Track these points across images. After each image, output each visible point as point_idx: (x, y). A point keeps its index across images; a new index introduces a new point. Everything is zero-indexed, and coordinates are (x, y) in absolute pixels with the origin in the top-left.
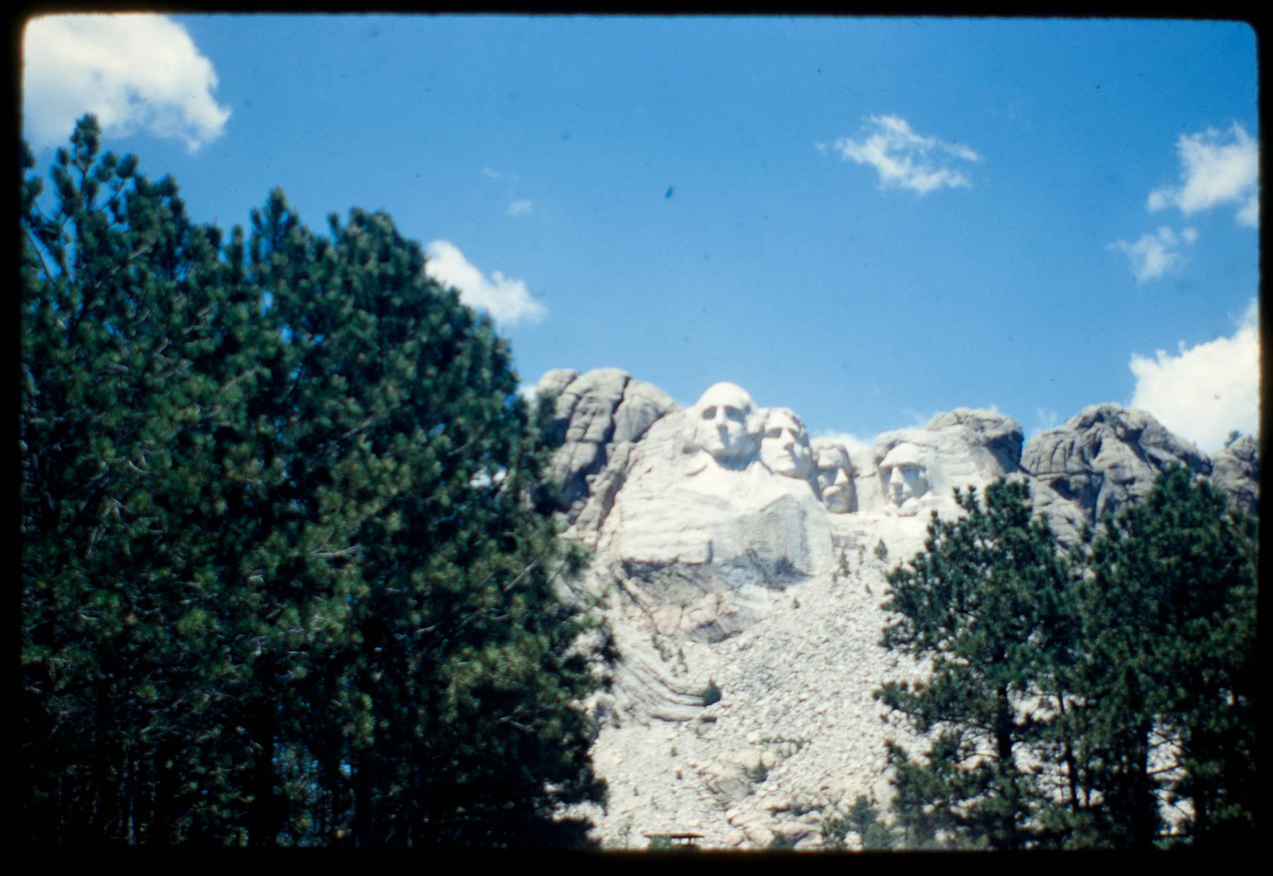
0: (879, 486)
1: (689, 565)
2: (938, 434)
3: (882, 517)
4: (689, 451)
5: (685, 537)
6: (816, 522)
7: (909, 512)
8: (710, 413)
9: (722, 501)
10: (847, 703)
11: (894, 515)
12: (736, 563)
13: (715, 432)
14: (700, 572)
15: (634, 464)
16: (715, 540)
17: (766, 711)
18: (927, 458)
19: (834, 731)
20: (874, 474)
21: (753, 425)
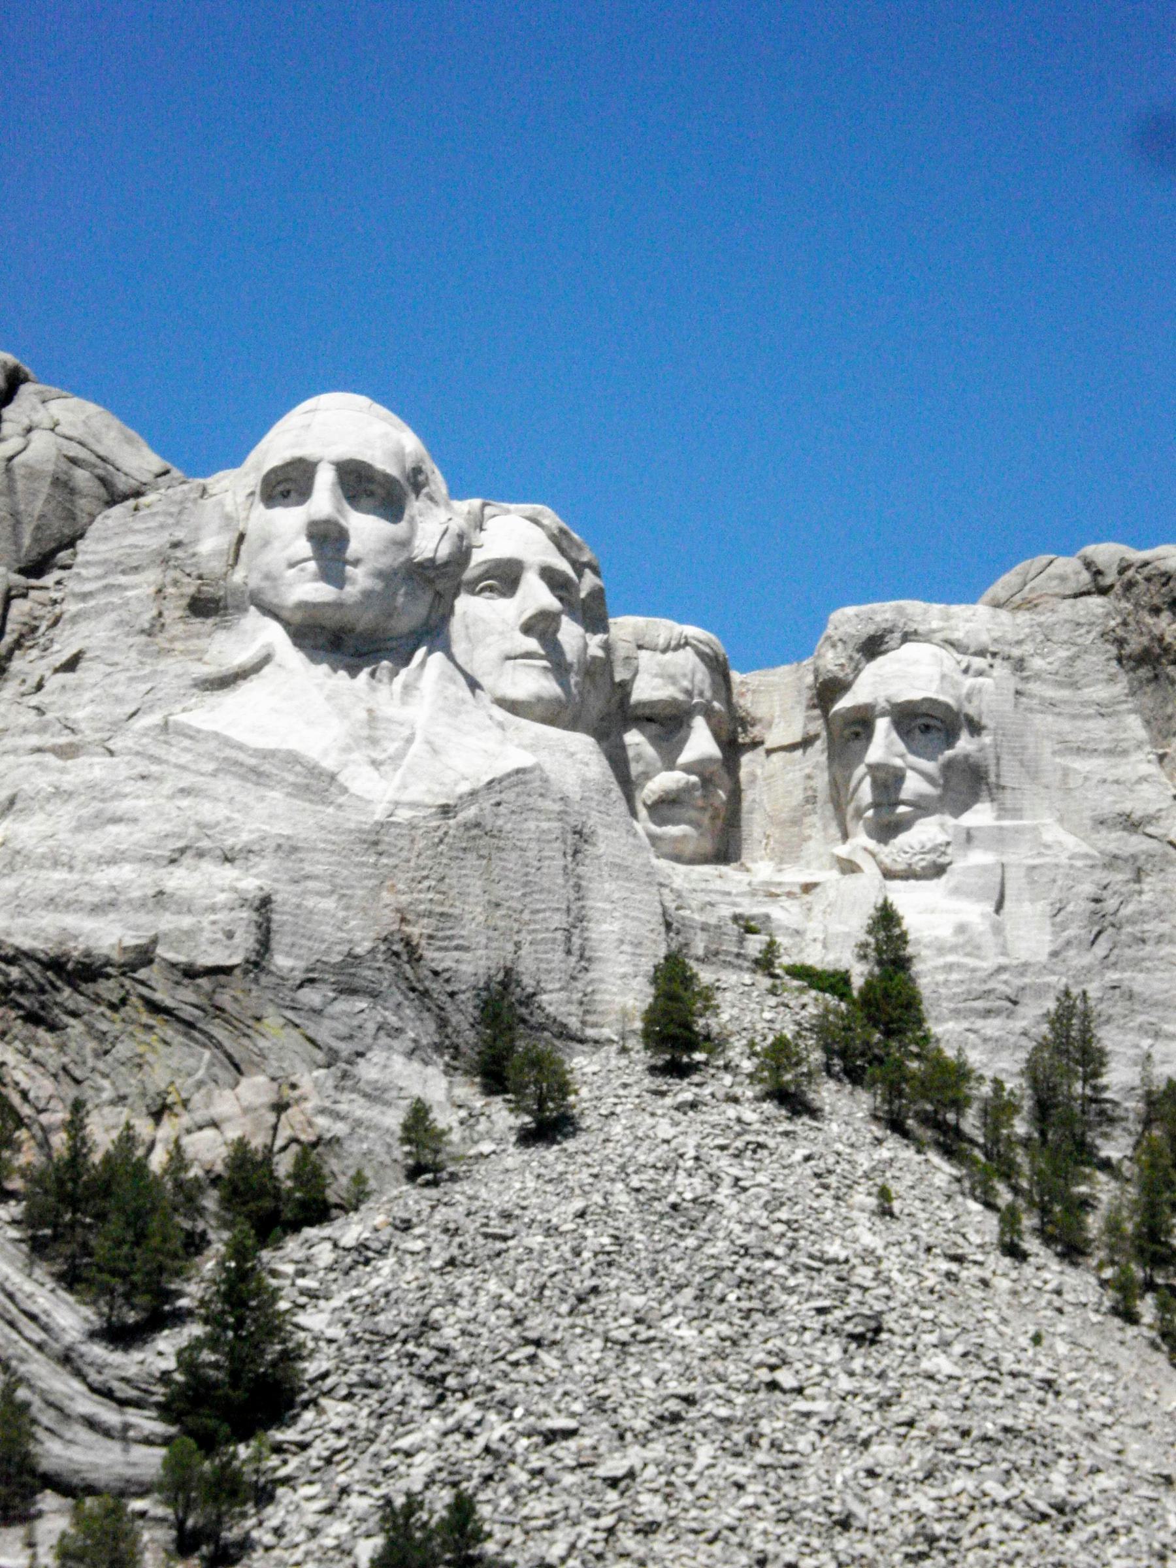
0: (822, 781)
1: (190, 973)
2: (1023, 617)
3: (830, 876)
4: (205, 606)
5: (178, 880)
6: (620, 869)
7: (920, 863)
8: (287, 484)
9: (314, 771)
10: (705, 1453)
11: (871, 870)
12: (347, 979)
13: (304, 548)
14: (224, 999)
15: (18, 644)
16: (284, 895)
18: (988, 693)
19: (659, 1544)
20: (806, 743)
21: (431, 529)
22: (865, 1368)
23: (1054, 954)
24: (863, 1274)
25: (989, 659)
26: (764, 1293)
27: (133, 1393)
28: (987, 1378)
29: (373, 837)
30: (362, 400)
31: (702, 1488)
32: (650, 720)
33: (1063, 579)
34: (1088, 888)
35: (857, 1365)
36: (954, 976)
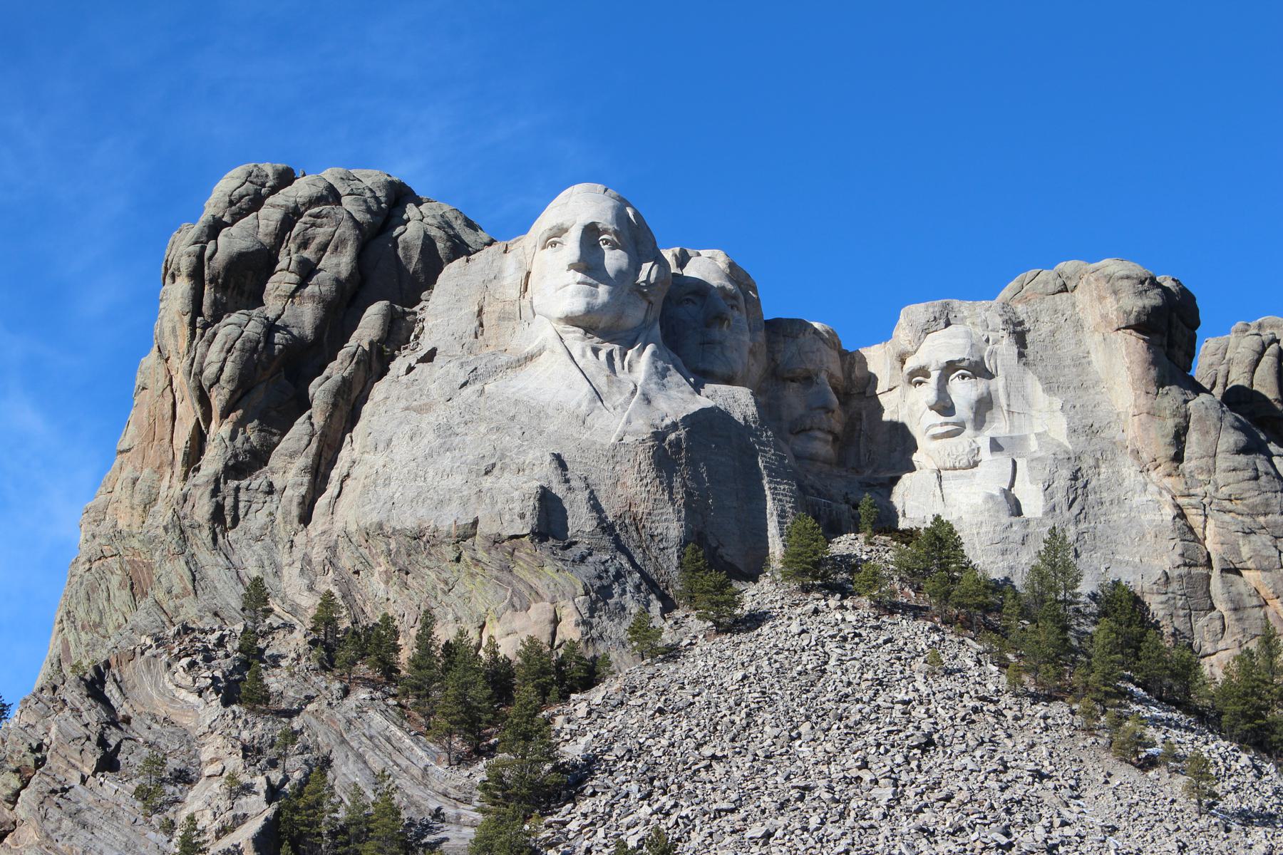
1: (497, 541)
17: (642, 831)
22: (919, 766)
23: (1046, 513)
24: (919, 712)
25: (1002, 333)
26: (857, 723)
27: (461, 795)
28: (995, 771)
29: (610, 454)
30: (600, 187)
31: (811, 842)
32: (793, 380)
33: (1046, 283)
34: (1065, 473)
35: (914, 764)
36: (983, 530)
